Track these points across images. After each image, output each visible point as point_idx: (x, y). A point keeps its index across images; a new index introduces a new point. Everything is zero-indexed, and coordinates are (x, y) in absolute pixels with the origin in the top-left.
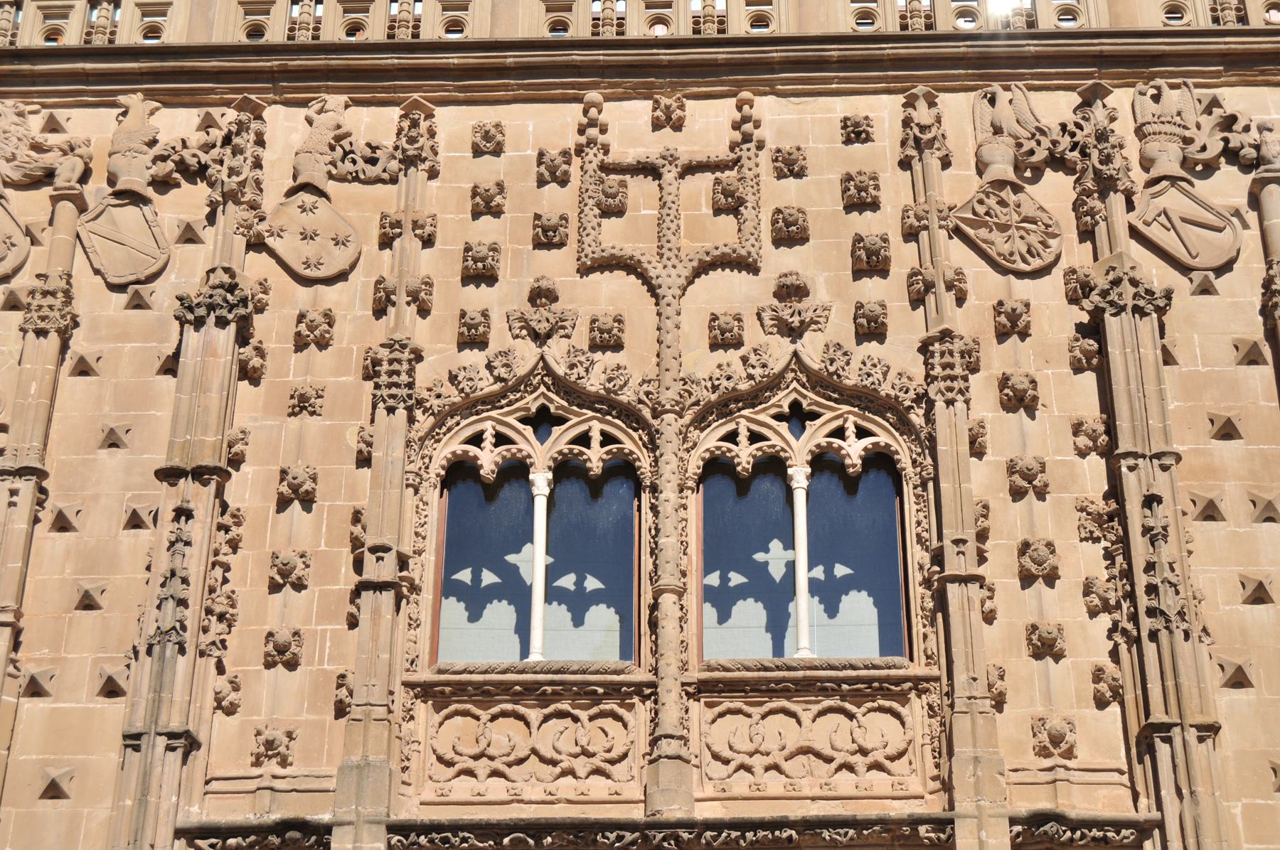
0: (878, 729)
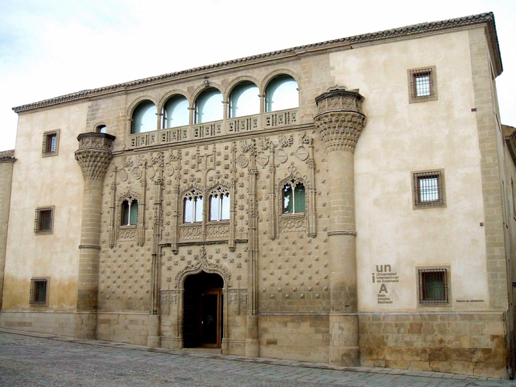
0: (226, 228)
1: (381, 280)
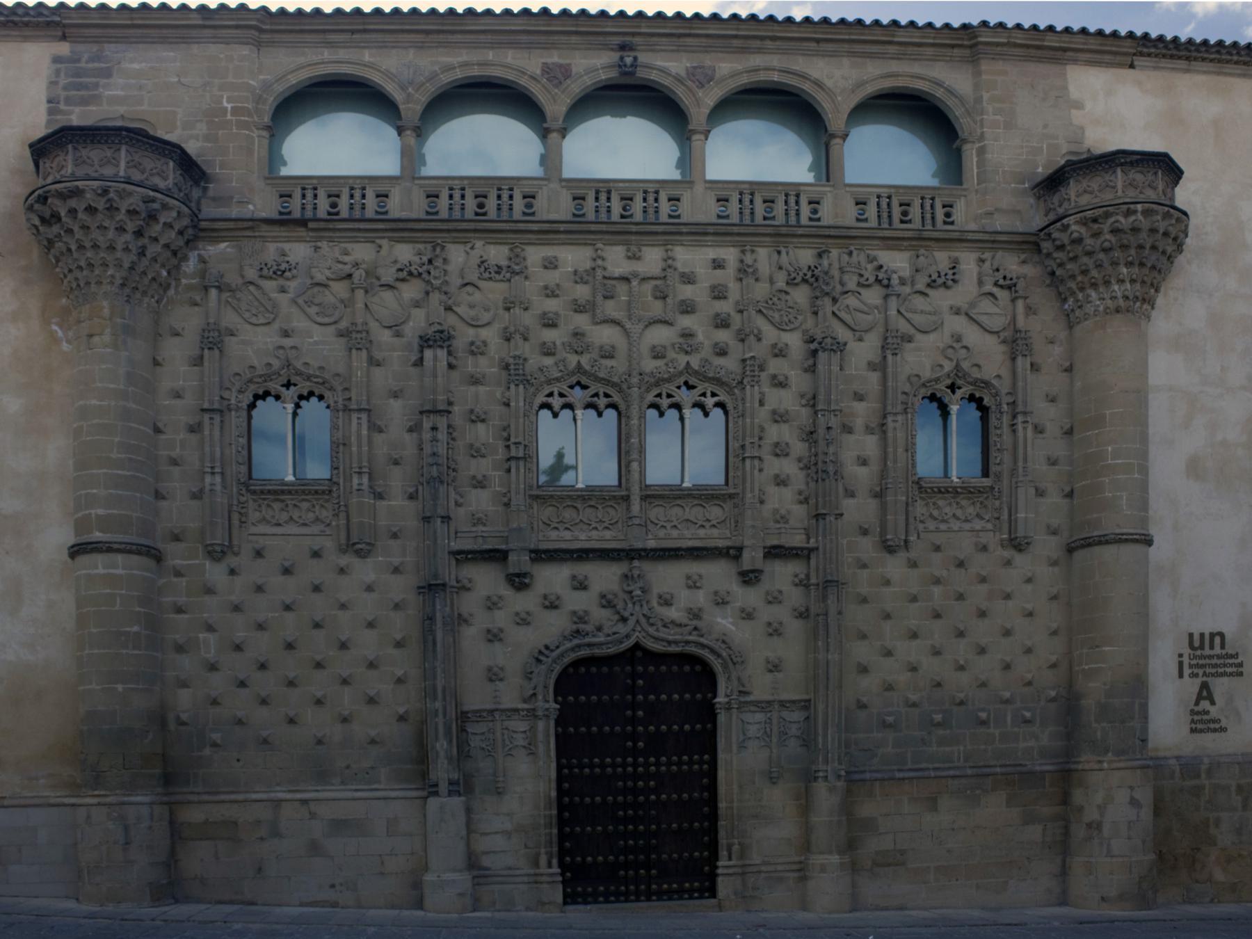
1: (1201, 672)
